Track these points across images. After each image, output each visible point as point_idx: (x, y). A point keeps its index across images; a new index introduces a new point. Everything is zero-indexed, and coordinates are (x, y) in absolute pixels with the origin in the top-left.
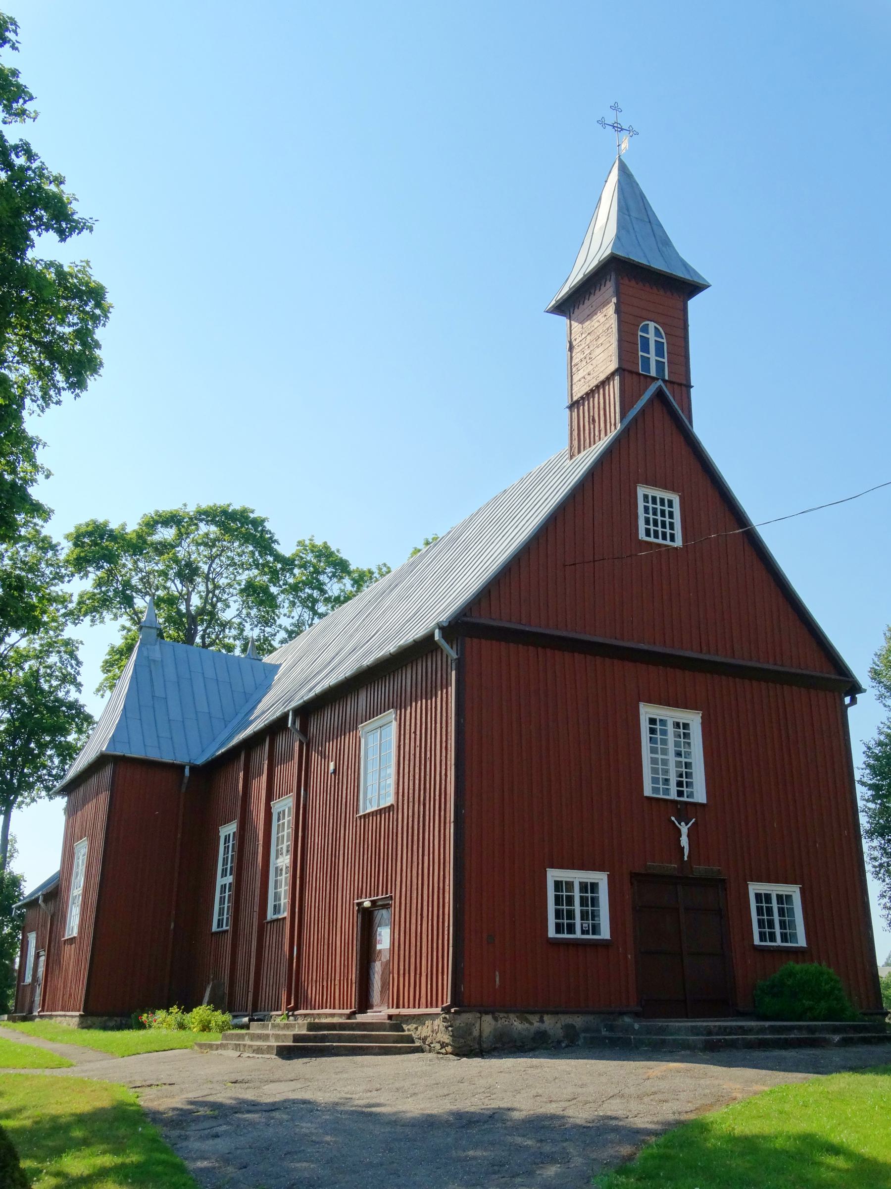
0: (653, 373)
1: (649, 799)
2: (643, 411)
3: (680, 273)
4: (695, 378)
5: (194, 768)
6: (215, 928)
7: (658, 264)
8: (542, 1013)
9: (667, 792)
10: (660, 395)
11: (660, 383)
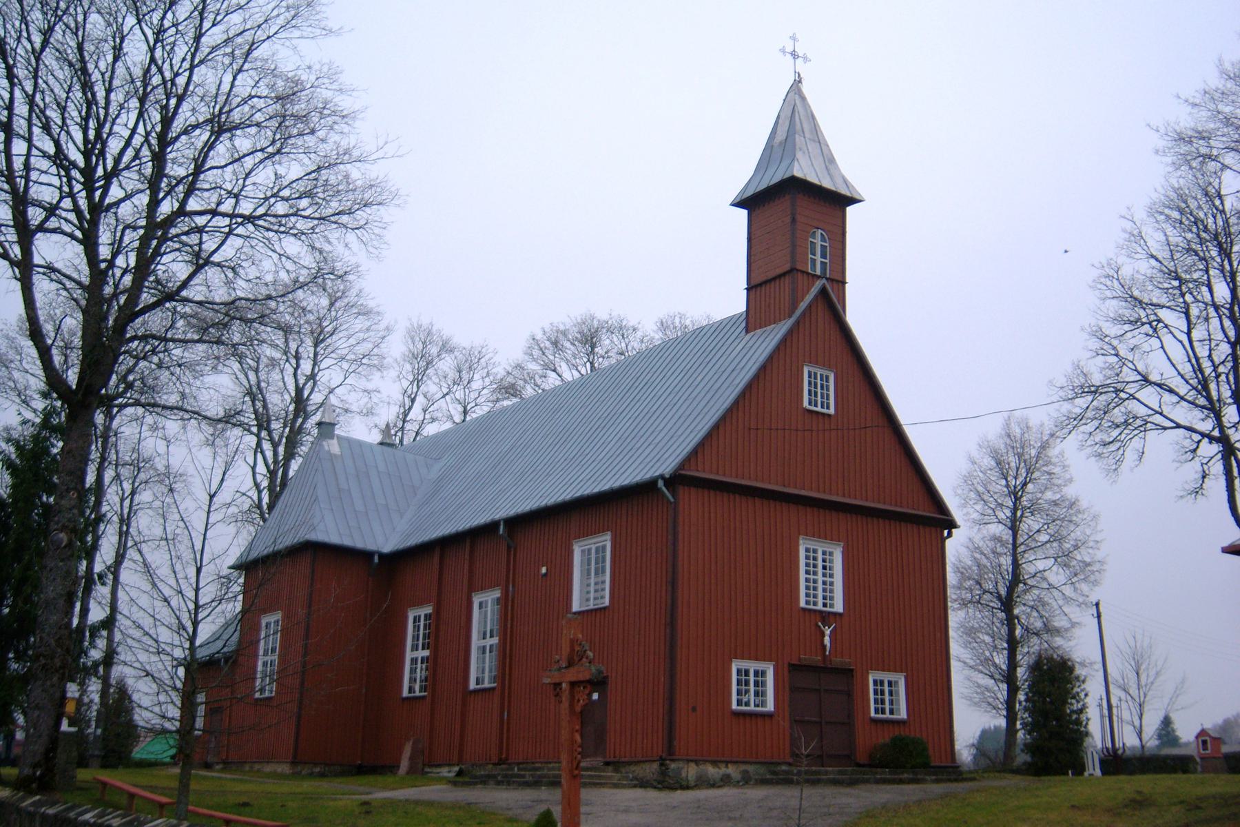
0: (818, 272)
1: (804, 610)
2: (810, 306)
3: (843, 191)
4: (849, 277)
5: (382, 556)
6: (405, 693)
7: (827, 184)
8: (727, 763)
9: (815, 604)
10: (823, 292)
11: (824, 281)
